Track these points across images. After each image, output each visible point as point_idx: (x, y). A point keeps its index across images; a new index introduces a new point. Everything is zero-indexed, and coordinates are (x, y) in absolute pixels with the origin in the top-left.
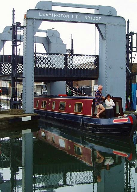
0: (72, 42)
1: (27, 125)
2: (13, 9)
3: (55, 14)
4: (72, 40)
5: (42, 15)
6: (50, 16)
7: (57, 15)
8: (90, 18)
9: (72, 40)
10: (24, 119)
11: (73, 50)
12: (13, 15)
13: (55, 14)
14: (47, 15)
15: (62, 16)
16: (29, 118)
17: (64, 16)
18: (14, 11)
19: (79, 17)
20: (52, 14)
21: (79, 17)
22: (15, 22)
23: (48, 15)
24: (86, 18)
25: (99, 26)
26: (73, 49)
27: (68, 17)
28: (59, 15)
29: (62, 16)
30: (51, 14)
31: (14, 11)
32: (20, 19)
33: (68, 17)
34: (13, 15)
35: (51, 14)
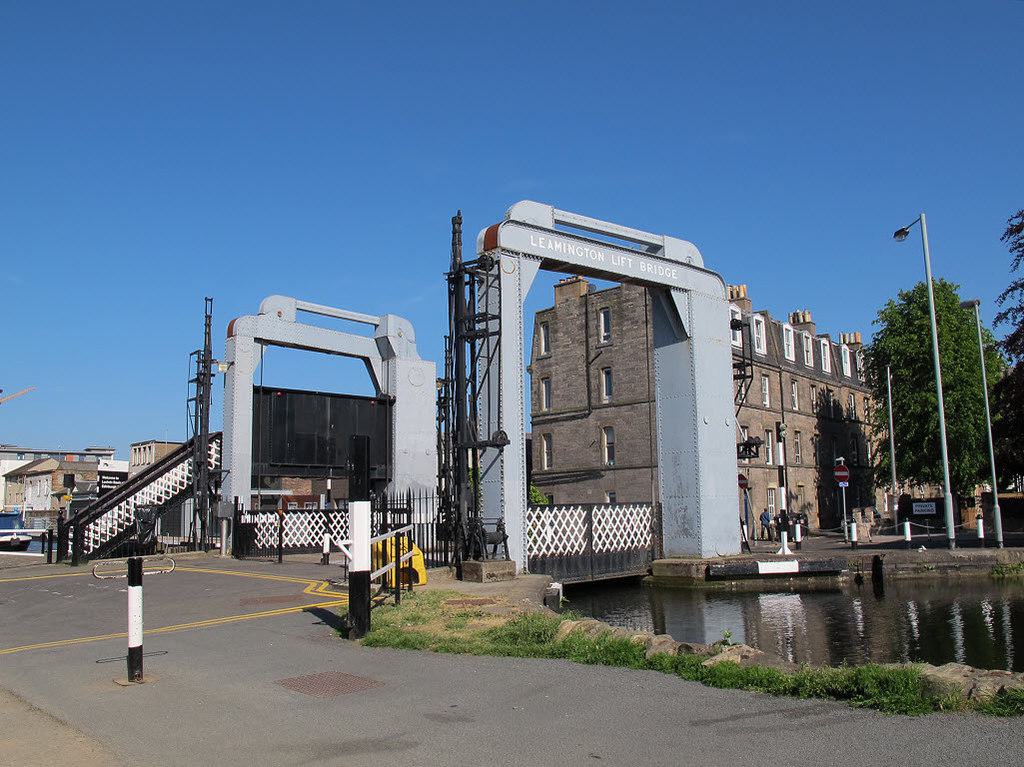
14: (550, 246)
18: (457, 221)
23: (554, 246)
25: (674, 293)
31: (457, 221)
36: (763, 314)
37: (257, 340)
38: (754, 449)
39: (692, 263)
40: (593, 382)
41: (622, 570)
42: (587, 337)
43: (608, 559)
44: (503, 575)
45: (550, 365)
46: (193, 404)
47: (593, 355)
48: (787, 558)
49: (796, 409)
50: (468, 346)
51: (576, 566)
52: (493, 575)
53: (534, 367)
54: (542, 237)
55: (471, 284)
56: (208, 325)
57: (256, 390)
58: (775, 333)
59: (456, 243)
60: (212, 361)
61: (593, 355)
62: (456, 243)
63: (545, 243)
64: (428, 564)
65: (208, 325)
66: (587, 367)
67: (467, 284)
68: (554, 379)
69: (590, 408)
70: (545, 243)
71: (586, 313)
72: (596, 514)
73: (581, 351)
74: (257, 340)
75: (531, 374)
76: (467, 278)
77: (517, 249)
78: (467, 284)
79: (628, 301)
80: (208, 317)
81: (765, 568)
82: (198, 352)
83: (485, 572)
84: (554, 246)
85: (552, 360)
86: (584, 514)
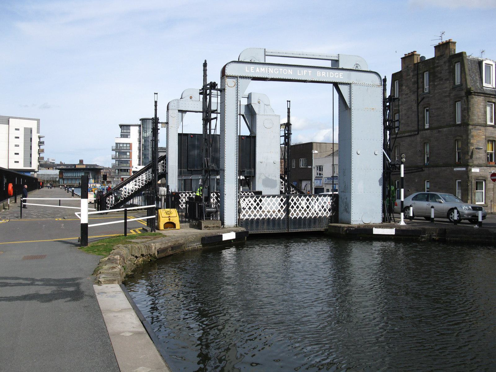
0: (289, 112)
1: (229, 244)
4: (289, 109)
8: (326, 74)
9: (289, 109)
10: (227, 237)
11: (291, 125)
12: (205, 71)
13: (270, 69)
14: (258, 70)
15: (282, 72)
16: (231, 236)
18: (205, 65)
19: (308, 73)
20: (265, 69)
21: (308, 73)
22: (208, 82)
23: (260, 70)
24: (319, 75)
25: (340, 86)
26: (292, 122)
27: (291, 73)
29: (282, 72)
30: (264, 68)
31: (205, 65)
32: (214, 77)
33: (291, 73)
34: (205, 71)
35: (264, 68)
37: (179, 111)
40: (420, 116)
41: (310, 228)
42: (418, 88)
43: (299, 221)
44: (214, 227)
47: (420, 99)
51: (279, 224)
54: (252, 67)
55: (210, 94)
56: (156, 106)
57: (180, 135)
61: (420, 99)
63: (255, 70)
64: (181, 222)
65: (156, 106)
66: (418, 106)
67: (208, 95)
69: (418, 131)
70: (255, 70)
71: (418, 74)
72: (292, 200)
73: (413, 97)
74: (179, 111)
76: (208, 92)
78: (208, 95)
79: (438, 66)
80: (156, 102)
83: (203, 226)
84: (260, 70)
86: (284, 200)
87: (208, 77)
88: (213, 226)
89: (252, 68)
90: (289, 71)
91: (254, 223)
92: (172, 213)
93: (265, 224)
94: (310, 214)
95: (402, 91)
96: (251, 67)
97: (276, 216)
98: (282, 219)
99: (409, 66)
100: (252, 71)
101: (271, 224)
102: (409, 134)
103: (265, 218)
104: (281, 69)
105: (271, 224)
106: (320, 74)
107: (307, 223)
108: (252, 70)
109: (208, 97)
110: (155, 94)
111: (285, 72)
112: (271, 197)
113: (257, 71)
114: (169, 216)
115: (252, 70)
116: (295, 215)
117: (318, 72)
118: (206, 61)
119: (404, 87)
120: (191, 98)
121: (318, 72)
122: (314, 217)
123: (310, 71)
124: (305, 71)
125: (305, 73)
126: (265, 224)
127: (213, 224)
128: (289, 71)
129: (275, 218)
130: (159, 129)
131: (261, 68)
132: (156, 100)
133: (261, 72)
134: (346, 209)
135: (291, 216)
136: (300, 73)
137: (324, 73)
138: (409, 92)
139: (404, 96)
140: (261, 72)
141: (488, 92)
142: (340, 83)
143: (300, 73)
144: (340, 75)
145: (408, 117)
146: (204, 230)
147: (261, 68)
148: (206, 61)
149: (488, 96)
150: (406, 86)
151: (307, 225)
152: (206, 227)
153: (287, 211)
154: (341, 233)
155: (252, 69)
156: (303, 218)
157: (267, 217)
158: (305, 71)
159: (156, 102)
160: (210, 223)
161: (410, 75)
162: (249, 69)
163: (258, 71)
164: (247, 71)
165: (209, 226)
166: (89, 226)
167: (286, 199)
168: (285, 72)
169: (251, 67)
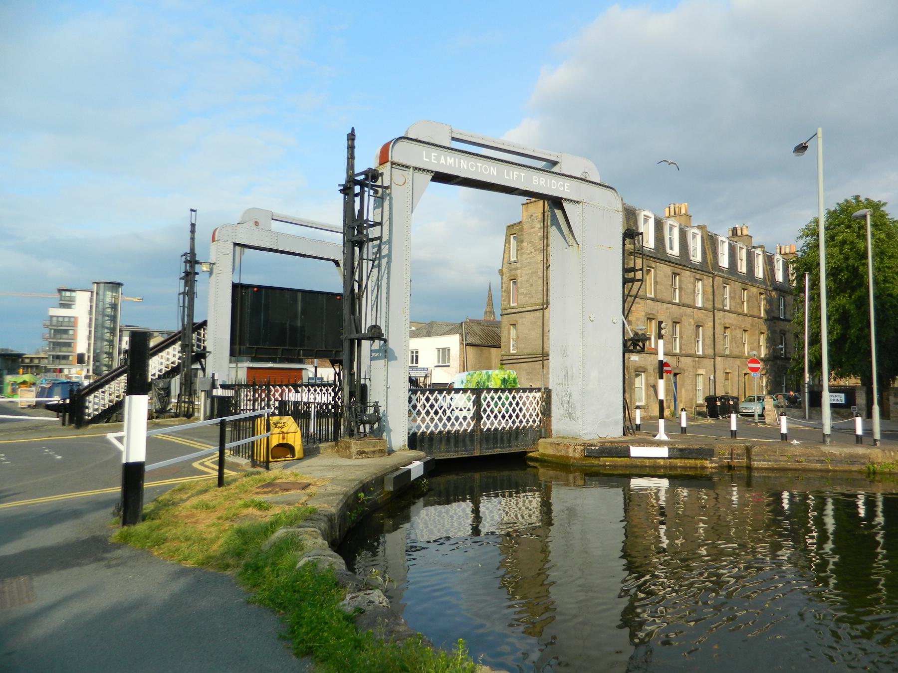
2: (350, 131)
3: (462, 161)
5: (430, 159)
6: (450, 165)
7: (468, 165)
8: (546, 183)
12: (351, 148)
13: (462, 161)
14: (442, 161)
15: (481, 167)
17: (486, 170)
18: (351, 137)
19: (519, 177)
21: (519, 177)
23: (446, 161)
24: (536, 182)
25: (566, 205)
27: (495, 174)
28: (472, 166)
30: (453, 159)
31: (351, 137)
33: (495, 174)
34: (351, 148)
35: (453, 159)
36: (701, 228)
38: (641, 344)
39: (588, 179)
41: (510, 446)
43: (494, 436)
44: (374, 452)
45: (516, 269)
46: (181, 296)
48: (659, 444)
49: (727, 308)
50: (357, 249)
51: (464, 441)
52: (364, 452)
53: (505, 270)
54: (434, 153)
55: (361, 194)
57: (235, 287)
58: (710, 242)
59: (351, 157)
60: (197, 263)
62: (351, 157)
63: (438, 158)
68: (519, 280)
70: (438, 158)
75: (502, 275)
76: (357, 189)
77: (408, 164)
78: (357, 195)
81: (636, 451)
82: (186, 254)
84: (446, 161)
85: (518, 265)
86: (473, 398)
87: (356, 162)
88: (372, 449)
89: (434, 156)
90: (492, 169)
91: (426, 440)
92: (286, 425)
93: (443, 442)
94: (524, 423)
95: (522, 249)
96: (433, 154)
97: (436, 429)
98: (468, 431)
99: (534, 215)
100: (433, 161)
101: (452, 441)
102: (534, 308)
103: (443, 431)
104: (479, 165)
105: (452, 441)
106: (537, 181)
107: (505, 438)
108: (434, 160)
109: (357, 200)
110: (192, 210)
111: (486, 169)
112: (461, 392)
113: (441, 162)
114: (283, 432)
115: (434, 160)
116: (488, 425)
117: (534, 177)
118: (353, 129)
119: (525, 244)
120: (256, 223)
121: (534, 177)
122: (495, 429)
123: (523, 174)
124: (515, 173)
125: (515, 176)
126: (443, 442)
127: (374, 447)
128: (492, 169)
129: (459, 431)
130: (197, 274)
131: (448, 158)
132: (193, 222)
133: (448, 164)
134: (569, 414)
135: (482, 427)
136: (508, 175)
137: (543, 180)
138: (533, 250)
139: (525, 256)
140: (448, 164)
141: (648, 254)
142: (565, 199)
143: (508, 175)
144: (566, 187)
145: (531, 285)
146: (356, 458)
147: (448, 158)
148: (353, 129)
149: (648, 258)
150: (529, 243)
151: (505, 442)
152: (361, 453)
153: (477, 417)
154: (571, 455)
155: (433, 158)
156: (500, 429)
157: (446, 430)
158: (515, 173)
159: (193, 225)
160: (368, 444)
161: (534, 227)
162: (429, 157)
163: (444, 162)
164: (425, 159)
165: (366, 450)
166: (147, 468)
167: (475, 396)
168: (486, 169)
169: (433, 154)
